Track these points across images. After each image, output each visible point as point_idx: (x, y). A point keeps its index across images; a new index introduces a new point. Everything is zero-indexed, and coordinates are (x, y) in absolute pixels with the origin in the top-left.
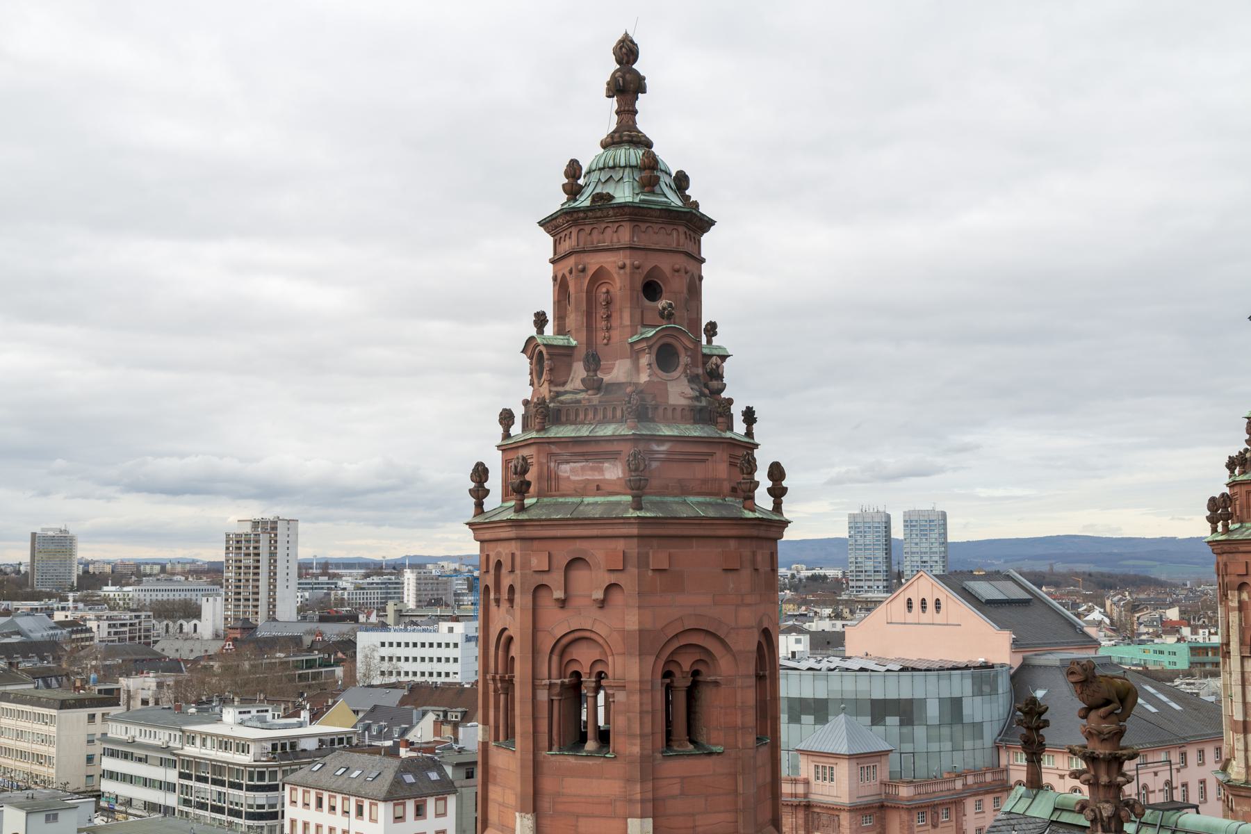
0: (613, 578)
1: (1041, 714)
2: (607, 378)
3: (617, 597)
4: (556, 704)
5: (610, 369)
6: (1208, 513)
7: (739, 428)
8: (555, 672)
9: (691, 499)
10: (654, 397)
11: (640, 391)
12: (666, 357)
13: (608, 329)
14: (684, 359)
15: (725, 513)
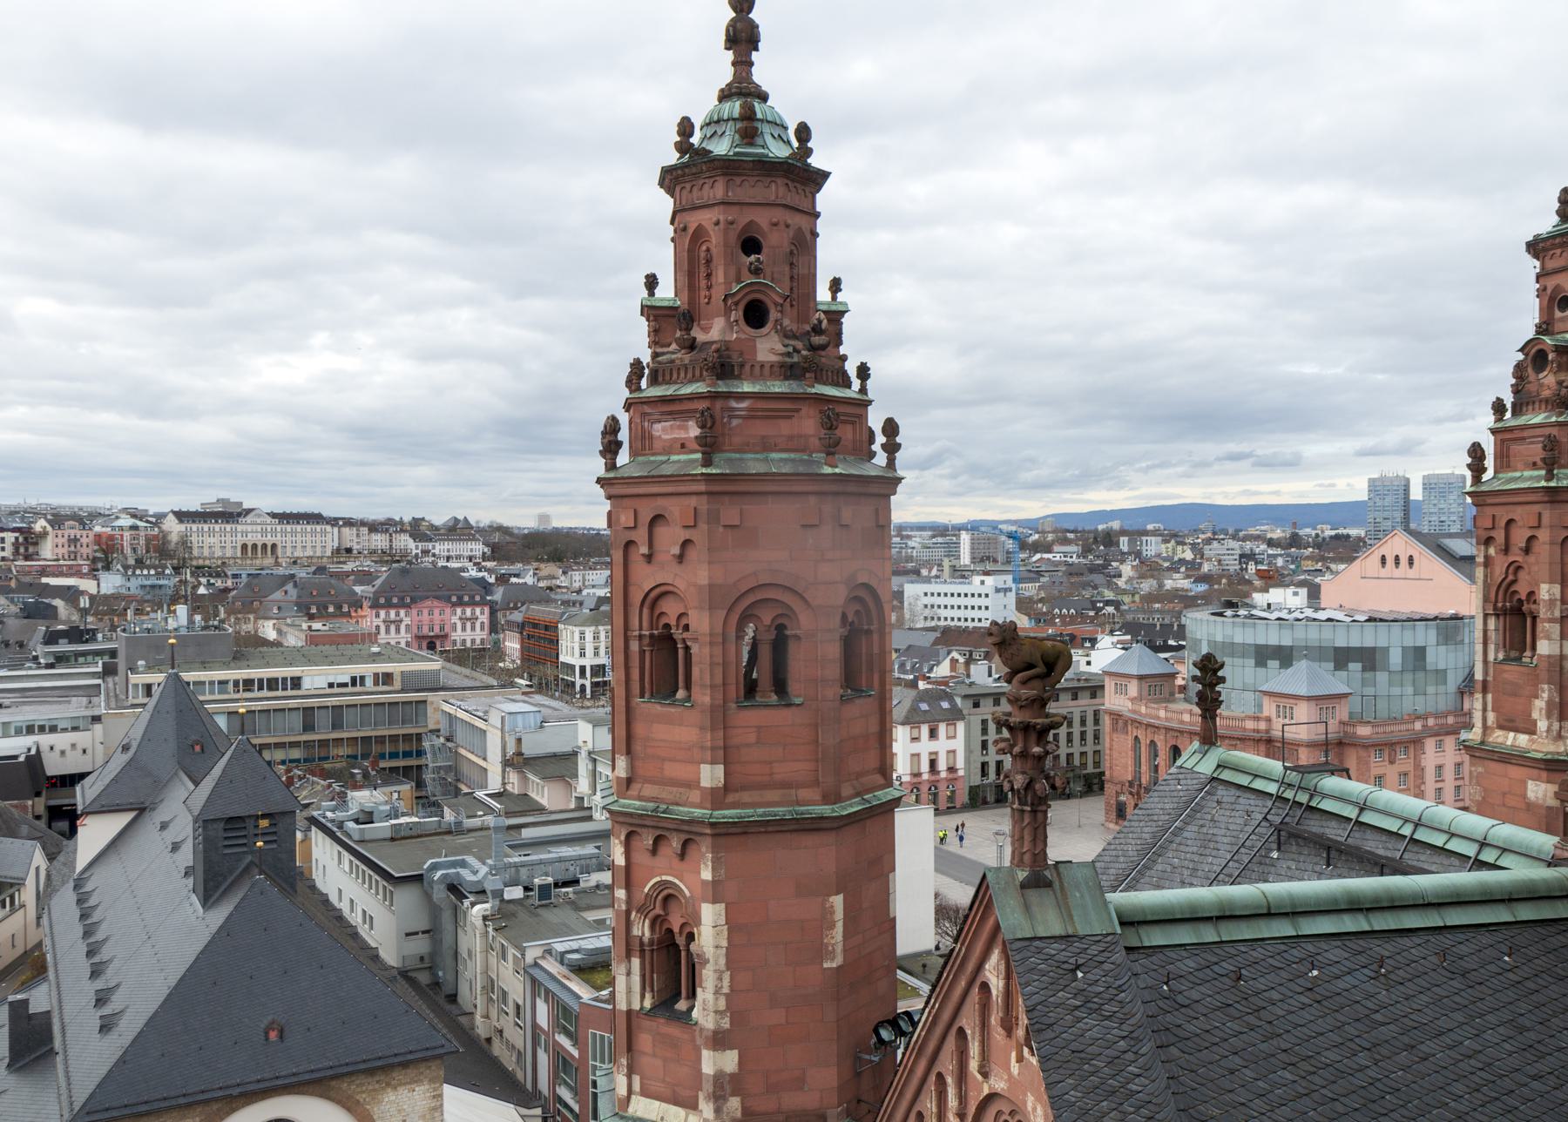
0: (686, 534)
1: (1215, 671)
2: (701, 337)
3: (692, 554)
4: (647, 655)
5: (706, 330)
6: (1469, 460)
7: (856, 384)
8: (645, 624)
9: (774, 455)
10: (742, 354)
11: (724, 349)
12: (755, 315)
13: (709, 288)
14: (773, 315)
15: (801, 469)
